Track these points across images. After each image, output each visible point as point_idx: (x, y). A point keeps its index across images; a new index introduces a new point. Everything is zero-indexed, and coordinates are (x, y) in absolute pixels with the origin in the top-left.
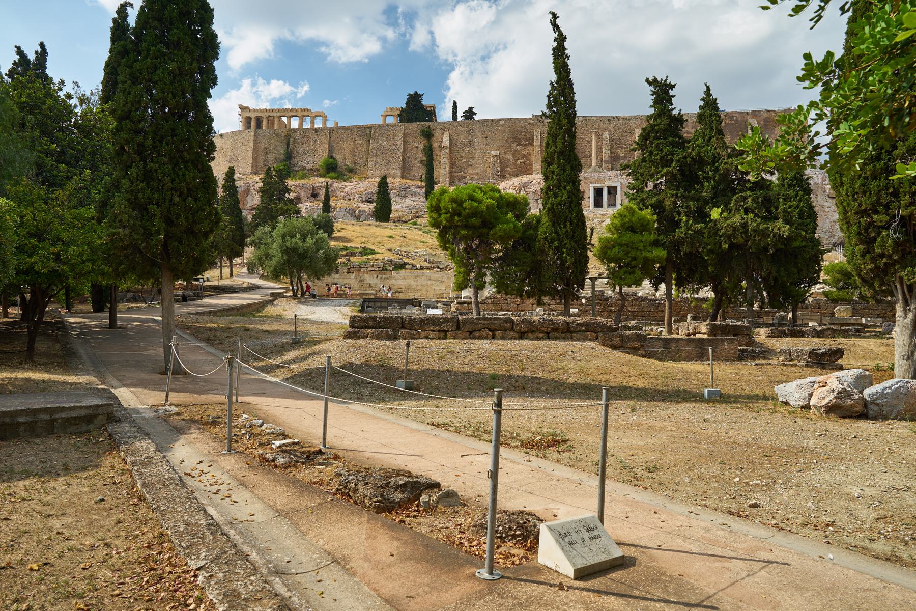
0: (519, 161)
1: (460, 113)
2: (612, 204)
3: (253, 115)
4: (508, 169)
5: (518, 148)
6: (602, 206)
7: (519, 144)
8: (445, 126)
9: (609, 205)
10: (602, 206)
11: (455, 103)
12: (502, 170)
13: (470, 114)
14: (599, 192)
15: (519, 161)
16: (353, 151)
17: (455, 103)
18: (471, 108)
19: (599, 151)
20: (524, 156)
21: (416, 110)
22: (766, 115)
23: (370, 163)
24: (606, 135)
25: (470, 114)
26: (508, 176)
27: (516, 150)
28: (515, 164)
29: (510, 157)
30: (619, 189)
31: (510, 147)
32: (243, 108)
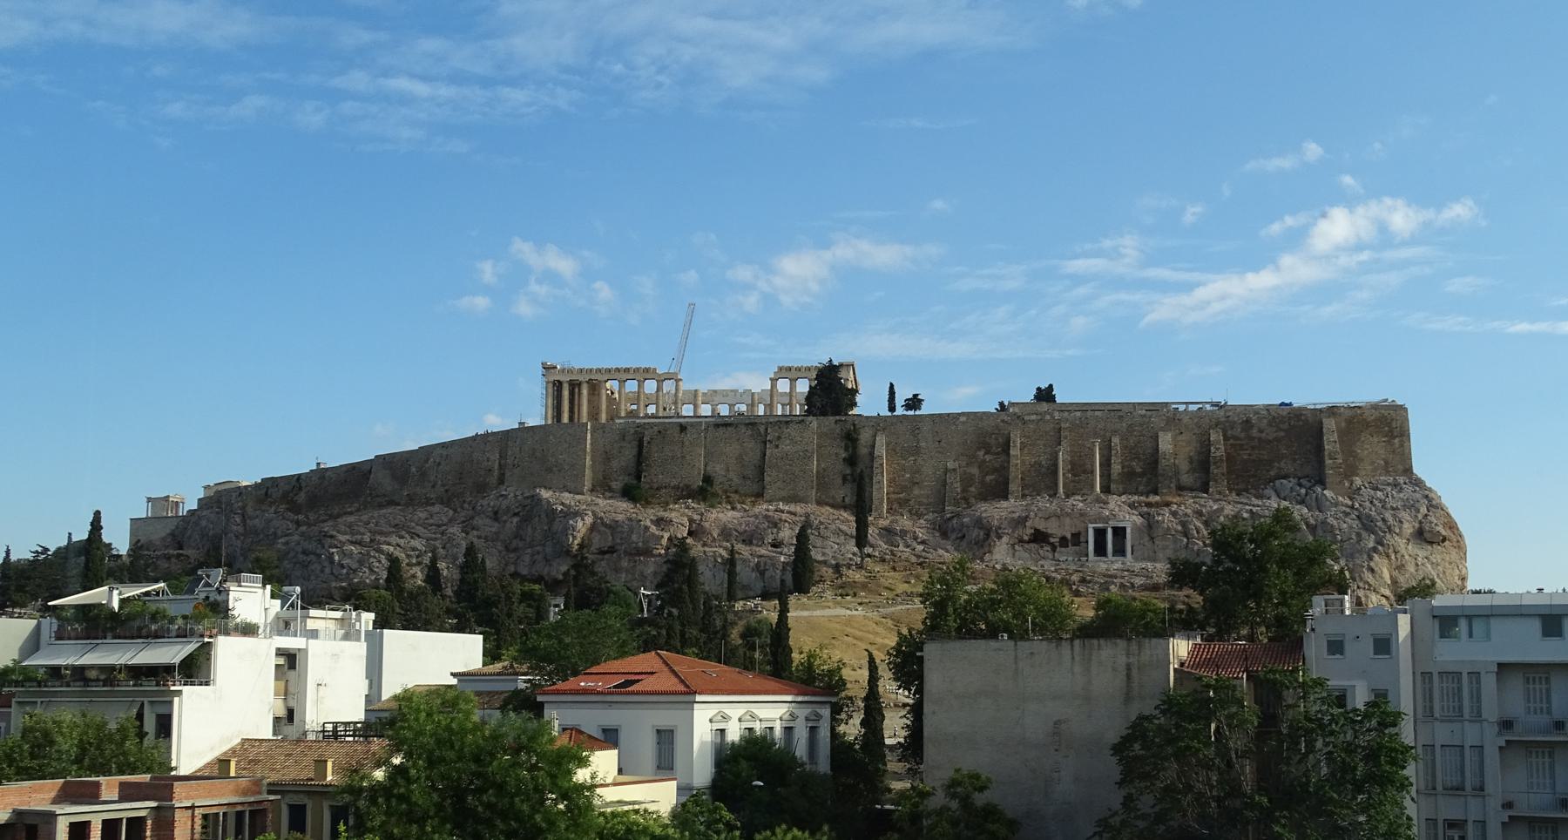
0: (988, 478)
1: (900, 401)
2: (1120, 551)
3: (565, 378)
5: (988, 457)
6: (1105, 554)
8: (877, 423)
10: (1105, 554)
11: (892, 386)
12: (964, 491)
13: (915, 402)
14: (1100, 534)
15: (988, 478)
16: (740, 458)
17: (892, 386)
18: (915, 396)
19: (1106, 464)
20: (995, 470)
21: (830, 389)
22: (1349, 413)
23: (767, 479)
24: (1116, 440)
25: (915, 402)
27: (984, 461)
28: (982, 482)
29: (975, 471)
30: (1128, 531)
32: (548, 368)
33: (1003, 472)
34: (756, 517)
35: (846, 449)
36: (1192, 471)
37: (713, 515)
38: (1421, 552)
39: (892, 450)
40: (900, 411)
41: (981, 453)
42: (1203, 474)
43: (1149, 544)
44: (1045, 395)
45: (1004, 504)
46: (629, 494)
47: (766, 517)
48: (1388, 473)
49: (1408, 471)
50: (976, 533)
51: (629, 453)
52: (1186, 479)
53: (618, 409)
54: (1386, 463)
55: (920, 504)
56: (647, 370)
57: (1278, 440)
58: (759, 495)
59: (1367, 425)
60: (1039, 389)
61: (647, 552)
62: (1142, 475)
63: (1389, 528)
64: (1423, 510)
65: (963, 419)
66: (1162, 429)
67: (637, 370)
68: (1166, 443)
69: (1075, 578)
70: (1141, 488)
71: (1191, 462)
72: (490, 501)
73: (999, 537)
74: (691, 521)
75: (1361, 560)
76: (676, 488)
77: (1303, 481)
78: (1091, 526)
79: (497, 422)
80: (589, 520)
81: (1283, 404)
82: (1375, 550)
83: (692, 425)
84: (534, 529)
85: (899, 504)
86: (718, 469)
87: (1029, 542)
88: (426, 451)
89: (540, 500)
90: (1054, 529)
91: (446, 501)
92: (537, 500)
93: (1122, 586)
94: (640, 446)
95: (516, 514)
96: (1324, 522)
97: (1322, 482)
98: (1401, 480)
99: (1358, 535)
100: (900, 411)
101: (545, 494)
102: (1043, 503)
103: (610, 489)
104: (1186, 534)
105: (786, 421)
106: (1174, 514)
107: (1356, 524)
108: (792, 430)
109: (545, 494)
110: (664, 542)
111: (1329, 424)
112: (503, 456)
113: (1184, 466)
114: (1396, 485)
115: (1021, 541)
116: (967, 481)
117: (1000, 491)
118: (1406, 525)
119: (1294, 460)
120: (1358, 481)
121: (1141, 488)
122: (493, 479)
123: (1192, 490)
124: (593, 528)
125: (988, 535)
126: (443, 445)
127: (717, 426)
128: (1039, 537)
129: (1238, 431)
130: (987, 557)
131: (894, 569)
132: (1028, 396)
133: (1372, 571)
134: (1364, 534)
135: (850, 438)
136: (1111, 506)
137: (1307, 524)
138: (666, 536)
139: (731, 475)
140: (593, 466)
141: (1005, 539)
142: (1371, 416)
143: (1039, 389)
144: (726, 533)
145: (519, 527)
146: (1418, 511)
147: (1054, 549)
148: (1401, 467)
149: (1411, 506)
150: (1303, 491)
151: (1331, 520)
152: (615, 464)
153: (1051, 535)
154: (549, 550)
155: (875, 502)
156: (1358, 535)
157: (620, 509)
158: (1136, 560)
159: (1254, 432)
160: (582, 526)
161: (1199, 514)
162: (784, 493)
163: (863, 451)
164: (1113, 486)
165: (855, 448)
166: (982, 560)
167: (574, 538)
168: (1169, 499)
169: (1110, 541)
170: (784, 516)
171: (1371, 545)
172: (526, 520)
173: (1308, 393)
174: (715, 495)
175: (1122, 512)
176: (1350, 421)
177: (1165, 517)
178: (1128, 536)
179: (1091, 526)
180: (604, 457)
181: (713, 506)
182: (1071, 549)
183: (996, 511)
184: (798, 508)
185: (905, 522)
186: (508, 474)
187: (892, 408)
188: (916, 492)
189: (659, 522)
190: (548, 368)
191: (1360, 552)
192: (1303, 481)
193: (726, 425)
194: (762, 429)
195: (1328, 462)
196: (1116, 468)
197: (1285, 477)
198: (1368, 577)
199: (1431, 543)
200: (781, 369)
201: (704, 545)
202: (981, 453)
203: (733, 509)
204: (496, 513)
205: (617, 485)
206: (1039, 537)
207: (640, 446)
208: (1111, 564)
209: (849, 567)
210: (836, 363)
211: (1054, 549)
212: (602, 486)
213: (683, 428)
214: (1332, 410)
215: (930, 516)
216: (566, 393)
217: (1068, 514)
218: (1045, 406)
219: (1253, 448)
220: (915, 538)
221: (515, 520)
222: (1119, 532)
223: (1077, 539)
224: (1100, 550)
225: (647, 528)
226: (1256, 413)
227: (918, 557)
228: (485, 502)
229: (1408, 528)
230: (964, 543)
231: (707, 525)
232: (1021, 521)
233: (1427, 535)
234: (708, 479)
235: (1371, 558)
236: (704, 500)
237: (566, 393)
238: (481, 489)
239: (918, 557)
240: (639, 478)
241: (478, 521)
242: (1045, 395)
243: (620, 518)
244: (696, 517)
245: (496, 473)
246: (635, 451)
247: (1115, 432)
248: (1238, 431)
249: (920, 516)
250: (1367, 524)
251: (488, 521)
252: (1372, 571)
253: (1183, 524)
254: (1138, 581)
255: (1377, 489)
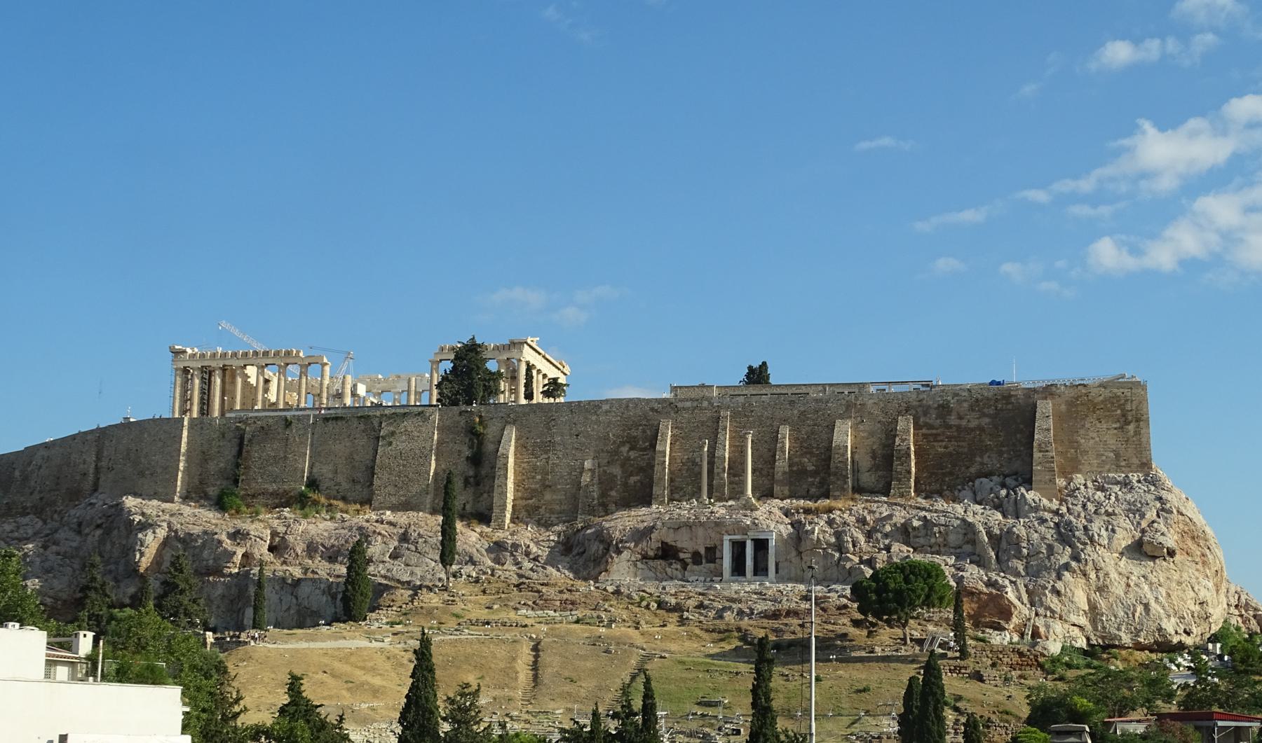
0: (633, 479)
1: (539, 386)
2: (760, 570)
4: (613, 493)
5: (633, 454)
7: (631, 449)
9: (756, 572)
14: (739, 547)
15: (633, 479)
16: (350, 458)
20: (641, 470)
22: (1069, 394)
23: (376, 482)
24: (785, 431)
26: (612, 507)
27: (628, 459)
28: (625, 484)
29: (616, 470)
30: (772, 543)
31: (616, 452)
33: (648, 470)
34: (350, 529)
35: (471, 447)
36: (875, 468)
37: (303, 526)
38: (1136, 569)
39: (521, 447)
40: (538, 398)
41: (625, 449)
42: (883, 473)
43: (795, 560)
44: (757, 376)
45: (644, 510)
46: (220, 504)
47: (360, 528)
48: (1118, 468)
49: (1145, 466)
50: (596, 548)
51: (229, 451)
52: (867, 479)
53: (254, 402)
54: (1117, 455)
55: (552, 512)
56: (288, 353)
57: (981, 428)
58: (367, 502)
59: (1093, 407)
60: (750, 368)
61: (218, 572)
62: (815, 473)
63: (1091, 539)
64: (1151, 514)
65: (606, 407)
66: (841, 417)
67: (277, 354)
68: (845, 436)
69: (691, 603)
70: (813, 490)
71: (874, 457)
72: (75, 513)
73: (619, 552)
74: (274, 534)
75: (1048, 580)
76: (274, 494)
77: (1009, 481)
78: (726, 538)
79: (111, 418)
80: (162, 533)
81: (992, 383)
82: (1067, 567)
83: (299, 419)
84: (113, 544)
85: (527, 513)
86: (325, 471)
87: (656, 557)
88: (31, 451)
89: (122, 509)
90: (684, 542)
91: (39, 511)
92: (119, 507)
93: (741, 613)
94: (241, 445)
95: (98, 526)
96: (1010, 532)
97: (1028, 483)
98: (1134, 477)
99: (1050, 548)
100: (538, 398)
101: (130, 502)
102: (685, 510)
103: (206, 496)
104: (840, 547)
105: (401, 414)
106: (830, 523)
107: (1050, 534)
108: (408, 424)
109: (130, 502)
110: (238, 558)
111: (1045, 408)
112: (99, 458)
113: (865, 462)
114: (1126, 484)
115: (645, 557)
116: (606, 483)
117: (645, 499)
118: (1120, 533)
119: (1000, 453)
120: (1079, 479)
121: (813, 490)
122: (87, 485)
123: (873, 492)
124: (166, 543)
125: (608, 550)
126: (46, 446)
127: (326, 419)
128: (667, 553)
129: (932, 418)
130: (602, 577)
131: (484, 592)
132: (737, 376)
133: (1058, 593)
134: (1058, 547)
135: (474, 435)
136: (758, 513)
137: (989, 533)
138: (240, 552)
139: (340, 478)
140: (187, 470)
141: (626, 554)
142: (1100, 395)
143: (750, 368)
144: (311, 549)
145: (102, 541)
146: (1143, 516)
147: (685, 565)
148: (1135, 461)
149: (1135, 511)
150: (1003, 492)
151: (1020, 530)
152: (212, 467)
153: (681, 550)
154: (121, 568)
155: (496, 510)
156: (1050, 548)
157: (200, 519)
158: (781, 580)
159: (953, 420)
160: (151, 542)
161: (862, 521)
162: (394, 500)
163: (490, 447)
164: (777, 489)
165: (481, 444)
166: (596, 581)
167: (142, 554)
168: (834, 504)
169: (752, 556)
170: (380, 528)
171: (1065, 559)
172: (108, 532)
173: (1021, 371)
174: (316, 503)
175: (771, 517)
176: (1071, 404)
177: (819, 529)
178: (772, 551)
179: (726, 538)
180: (200, 457)
181: (305, 516)
182: (706, 566)
183: (623, 522)
184: (402, 518)
185: (527, 535)
186: (103, 478)
187: (529, 396)
188: (548, 496)
189: (237, 536)
190: (177, 353)
191: (1047, 569)
192: (1009, 481)
193: (336, 419)
194: (376, 425)
195: (1037, 455)
196: (782, 465)
197: (988, 475)
198: (1052, 601)
199: (1153, 558)
200: (442, 349)
201: (284, 563)
202: (625, 449)
203: (332, 518)
204: (80, 524)
205: (213, 491)
206: (667, 553)
207: (241, 445)
208: (745, 588)
209: (430, 589)
210: (478, 341)
211: (685, 565)
212: (195, 494)
213: (288, 423)
214: (1049, 391)
215: (558, 528)
216: (218, 381)
217: (702, 524)
218: (752, 390)
219: (950, 438)
220: (527, 554)
221: (99, 532)
222: (761, 545)
223: (712, 554)
224: (738, 569)
225: (220, 542)
226: (956, 395)
227: (520, 576)
228: (73, 512)
229: (1124, 538)
230: (581, 561)
231: (290, 538)
232: (641, 535)
233: (1147, 548)
234: (313, 484)
235: (1059, 577)
236: (302, 508)
237: (218, 381)
238: (75, 495)
239: (520, 576)
240: (236, 482)
241: (61, 535)
242: (757, 376)
243: (196, 530)
244: (281, 529)
245: (91, 477)
246: (235, 451)
247: (785, 421)
248: (932, 418)
249: (547, 525)
250: (1065, 534)
251: (71, 535)
252: (1058, 593)
253: (838, 535)
254: (760, 607)
255: (1102, 489)
